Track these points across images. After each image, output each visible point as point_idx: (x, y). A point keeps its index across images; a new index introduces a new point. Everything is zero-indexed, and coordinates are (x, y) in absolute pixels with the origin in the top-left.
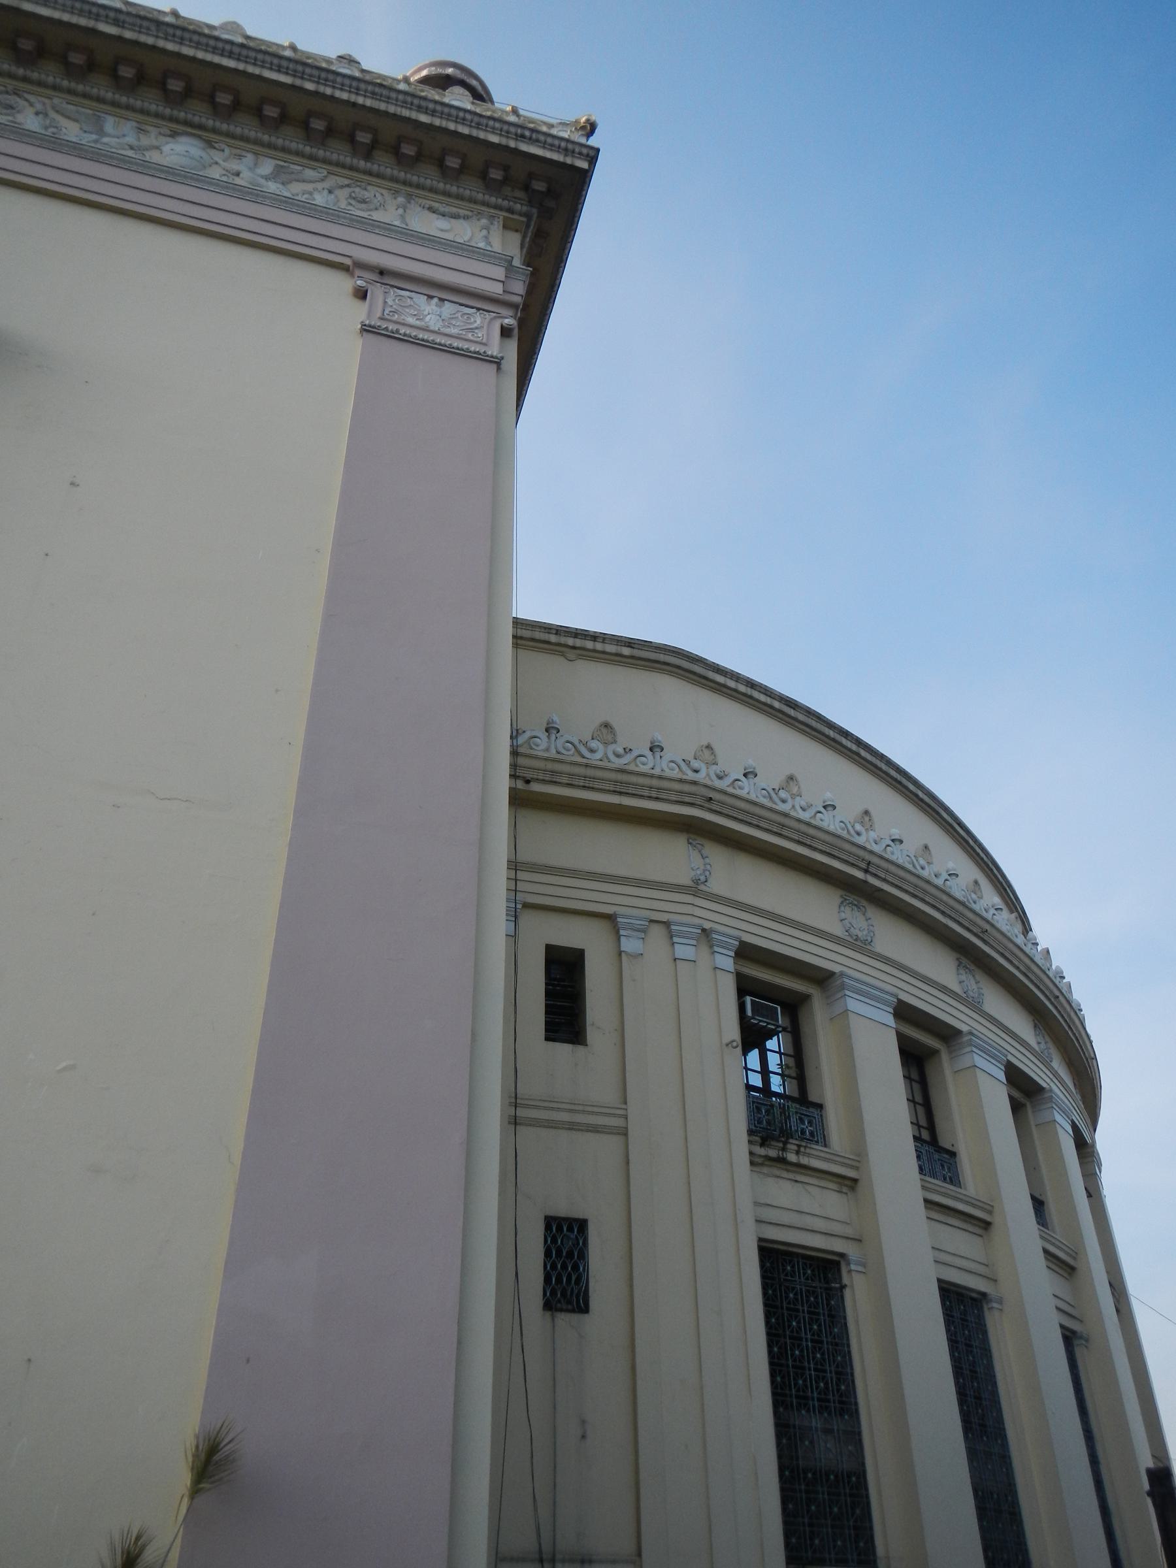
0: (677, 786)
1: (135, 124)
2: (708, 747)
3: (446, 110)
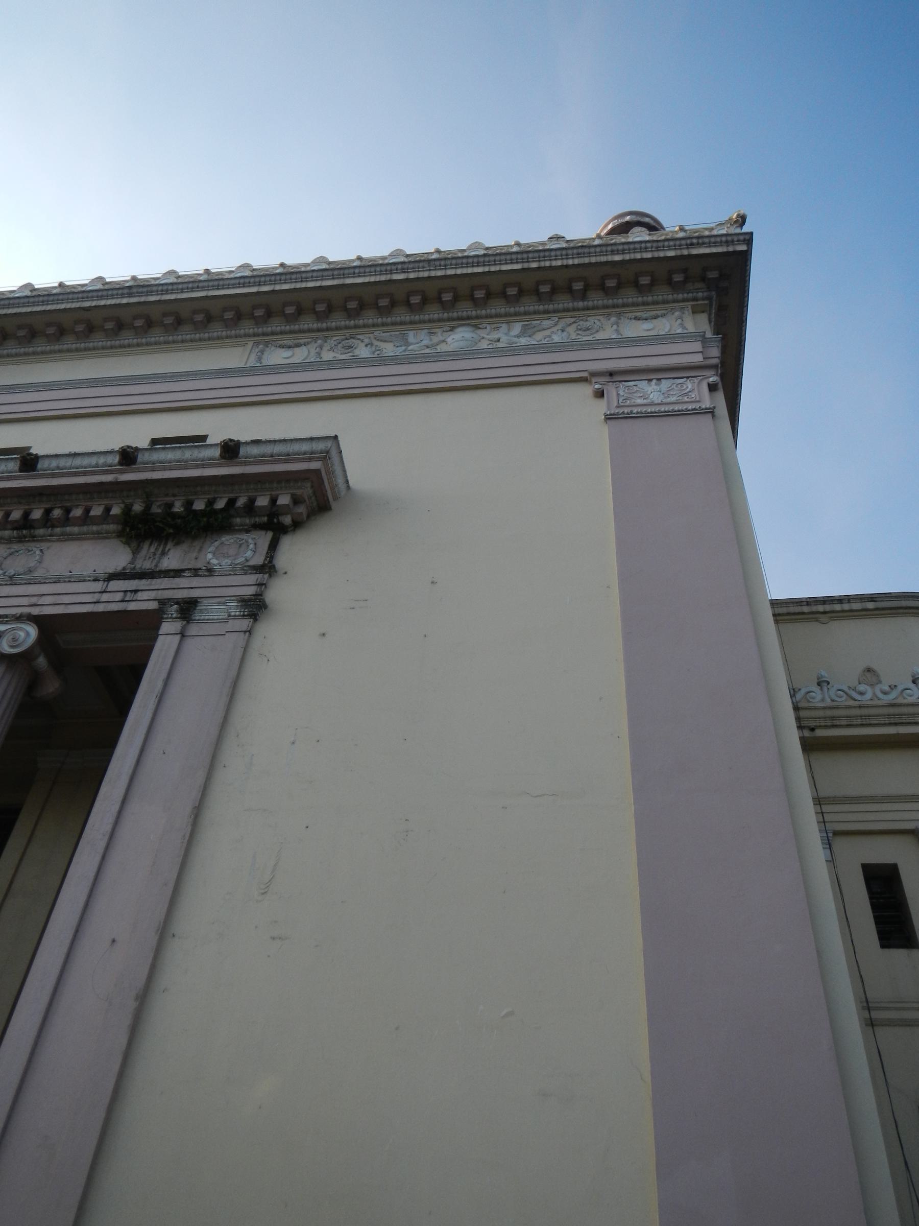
1: (426, 331)
3: (632, 246)
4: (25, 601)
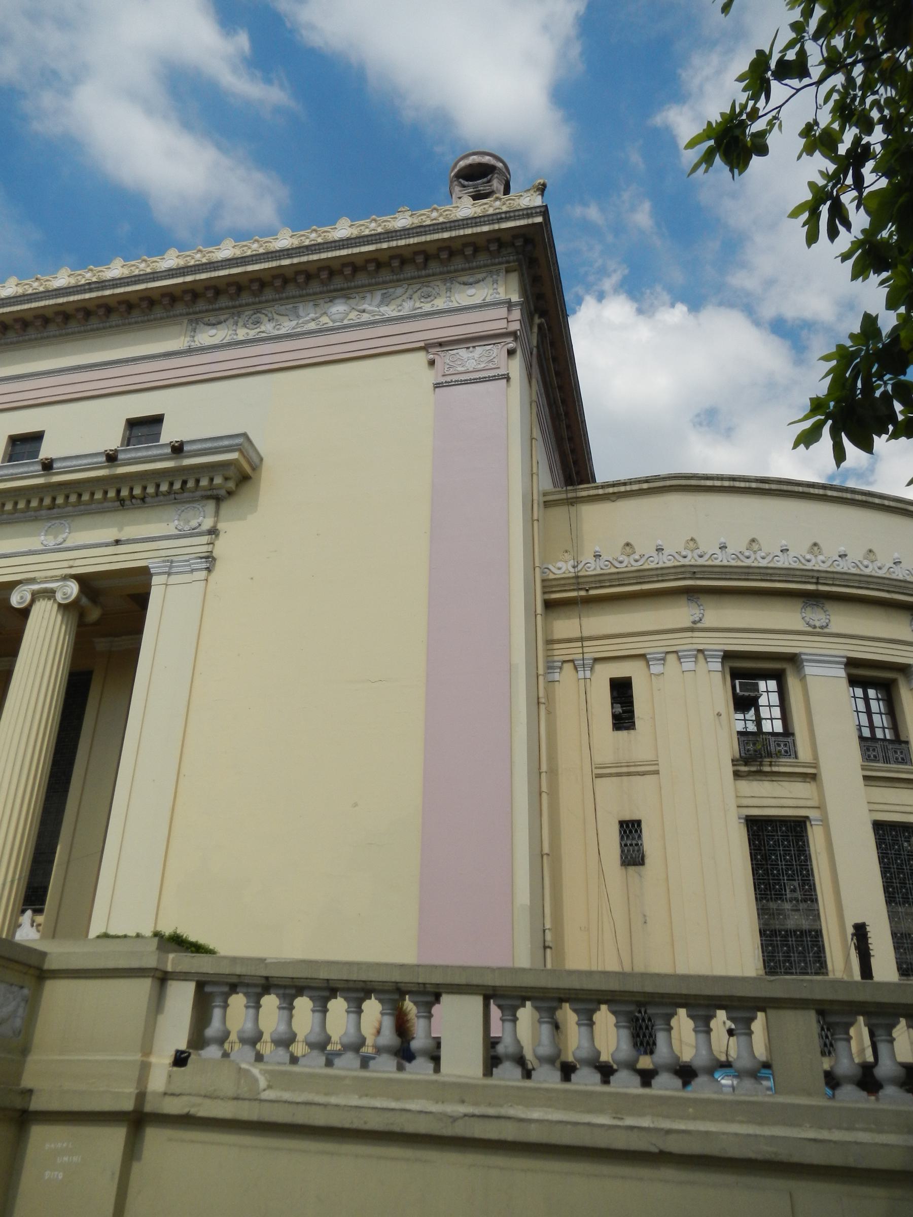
0: (673, 571)
1: (312, 303)
2: (692, 539)
3: (457, 224)
4: (66, 564)
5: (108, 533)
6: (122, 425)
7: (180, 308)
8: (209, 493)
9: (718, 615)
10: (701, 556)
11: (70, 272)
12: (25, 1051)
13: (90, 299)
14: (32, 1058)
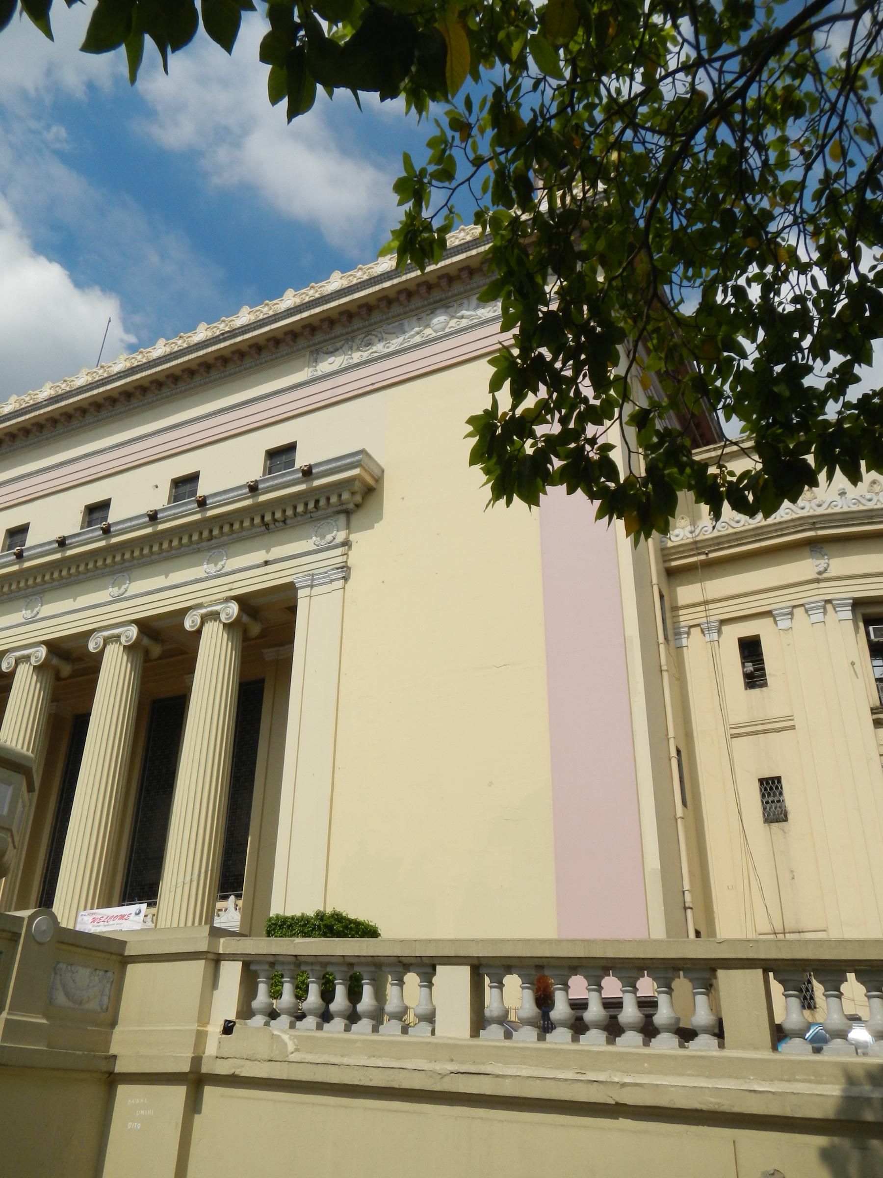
1: (415, 318)
5: (103, 596)
6: (262, 456)
7: (302, 343)
8: (339, 508)
9: (841, 564)
10: (819, 506)
11: (206, 326)
12: (113, 1024)
13: (225, 347)
14: (118, 1029)
